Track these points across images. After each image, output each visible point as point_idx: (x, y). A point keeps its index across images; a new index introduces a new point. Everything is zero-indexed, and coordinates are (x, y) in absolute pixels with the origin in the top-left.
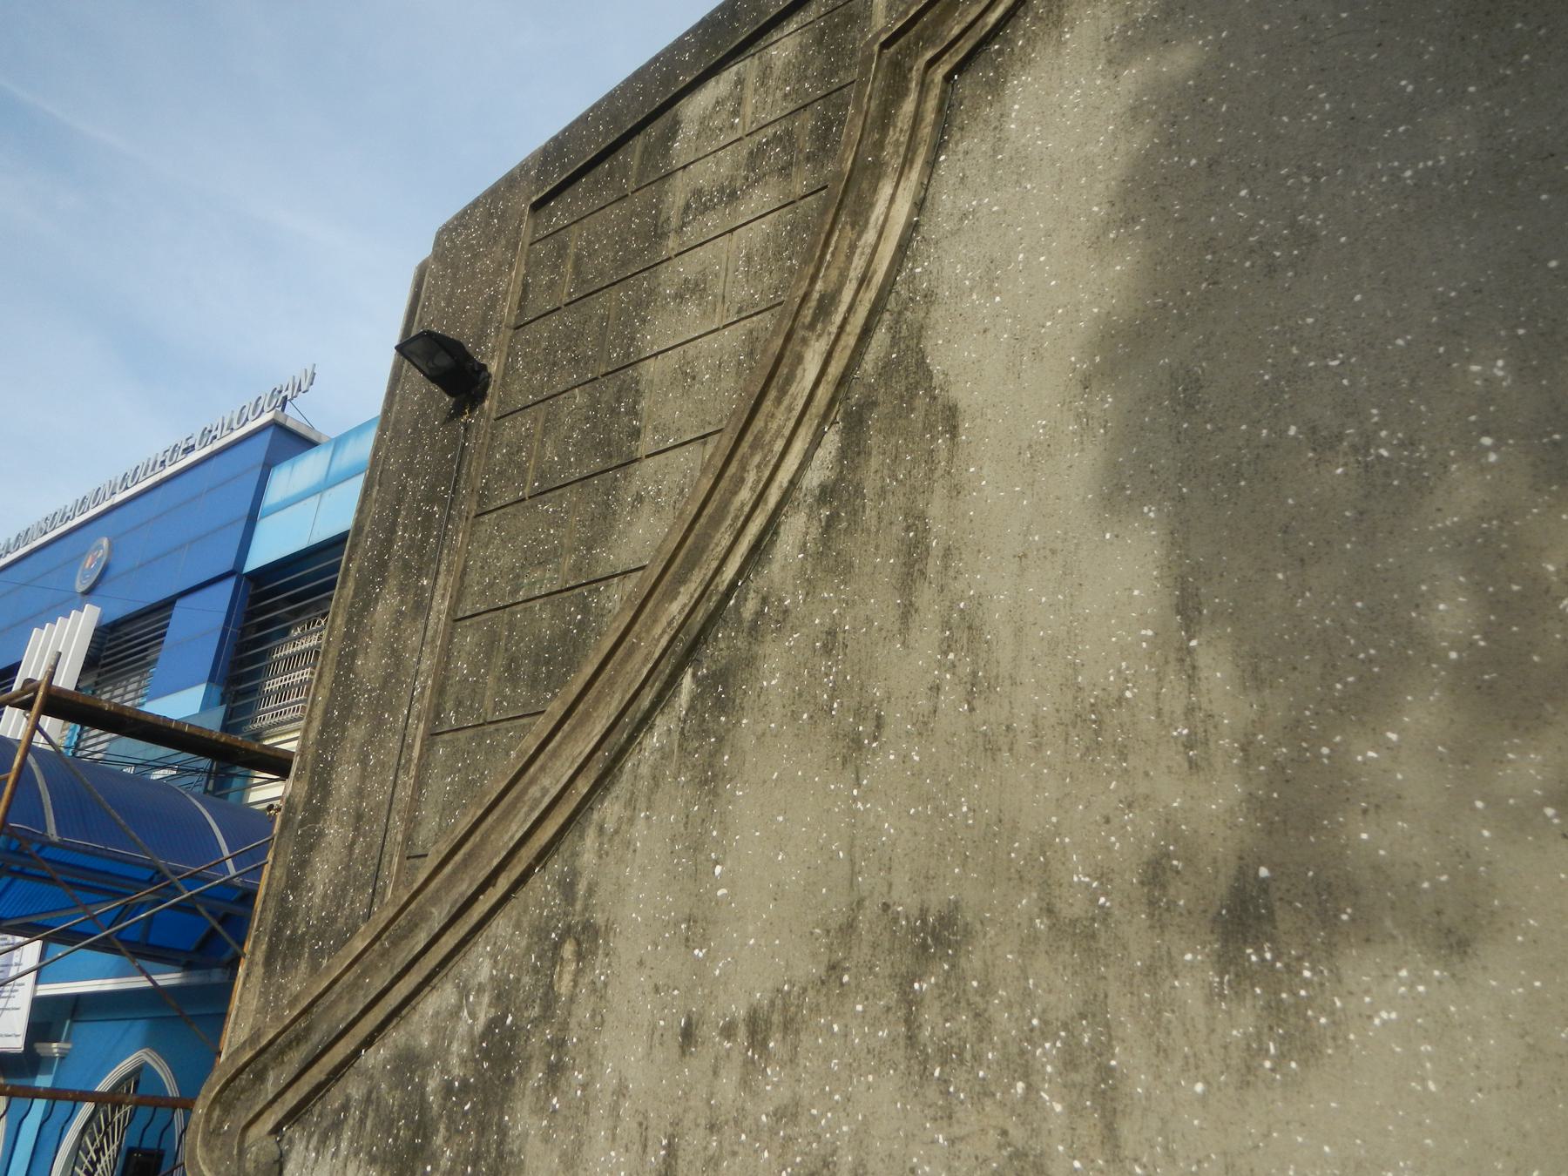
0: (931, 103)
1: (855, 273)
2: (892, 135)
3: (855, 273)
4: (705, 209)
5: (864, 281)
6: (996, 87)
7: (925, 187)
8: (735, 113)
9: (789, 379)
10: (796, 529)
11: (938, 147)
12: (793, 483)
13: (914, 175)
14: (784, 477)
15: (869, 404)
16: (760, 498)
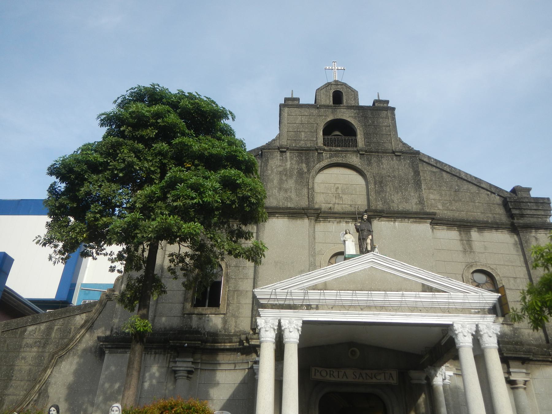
0: (55, 361)
1: (43, 379)
2: (51, 363)
3: (43, 379)
4: (27, 347)
5: (44, 379)
6: (61, 362)
7: (52, 370)
8: (34, 334)
9: (35, 388)
10: (32, 403)
11: (55, 366)
12: (33, 399)
13: (52, 369)
14: (32, 398)
15: (41, 393)
16: (29, 400)
